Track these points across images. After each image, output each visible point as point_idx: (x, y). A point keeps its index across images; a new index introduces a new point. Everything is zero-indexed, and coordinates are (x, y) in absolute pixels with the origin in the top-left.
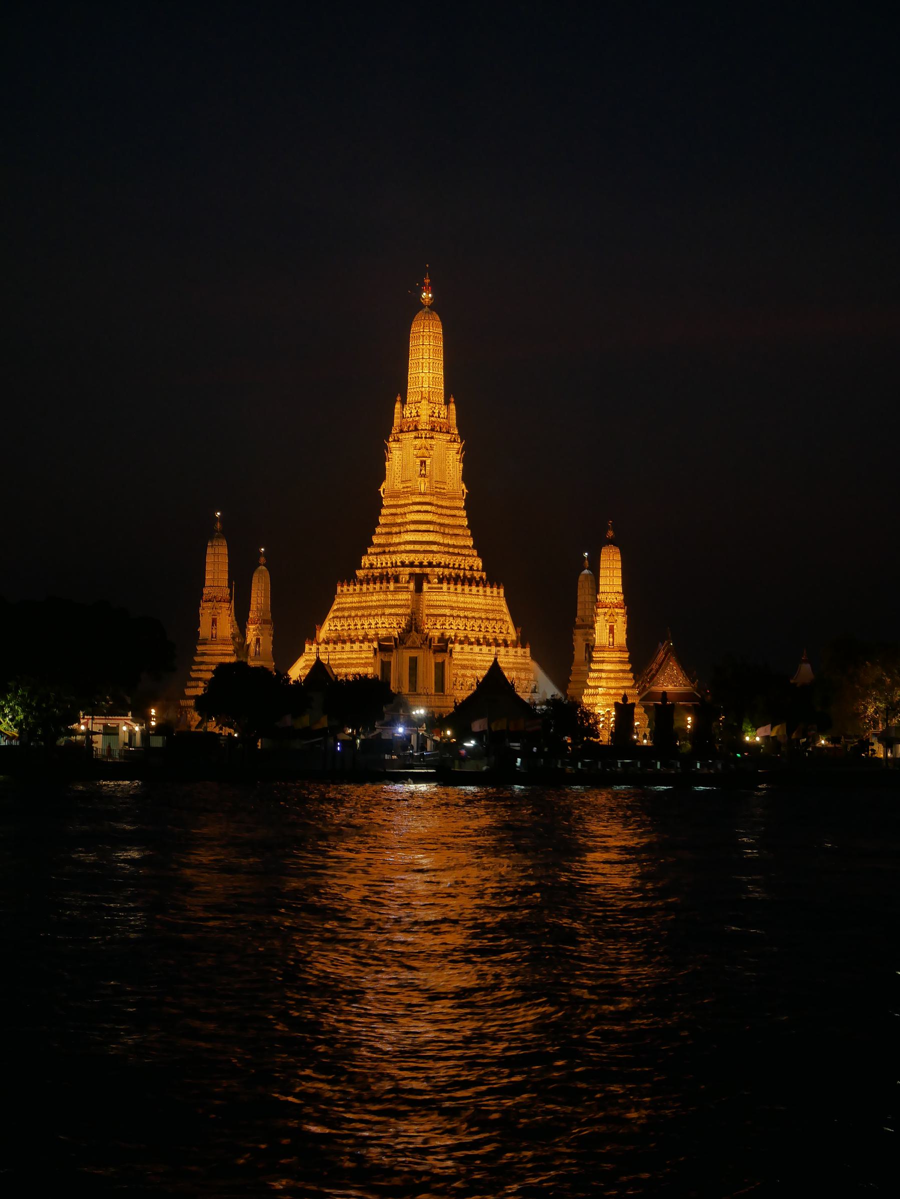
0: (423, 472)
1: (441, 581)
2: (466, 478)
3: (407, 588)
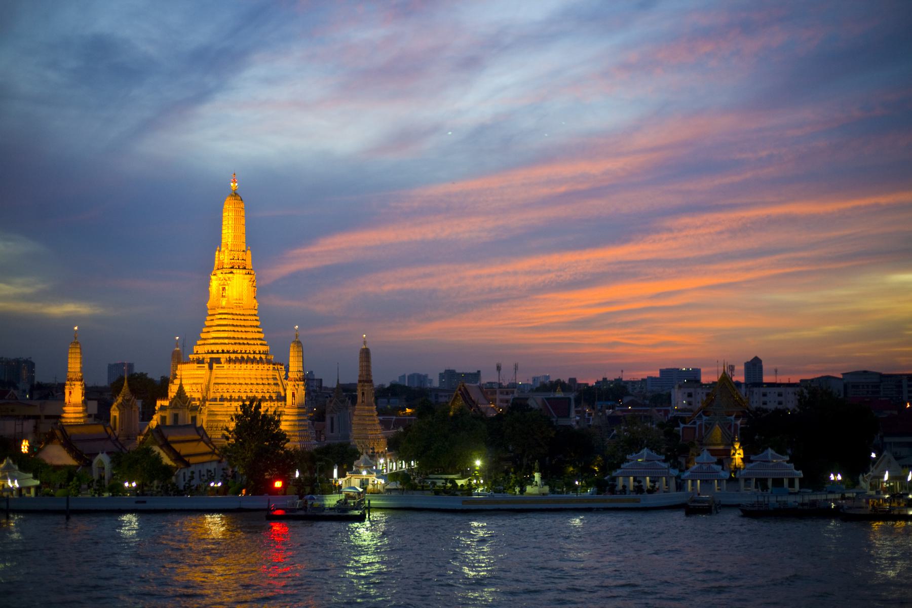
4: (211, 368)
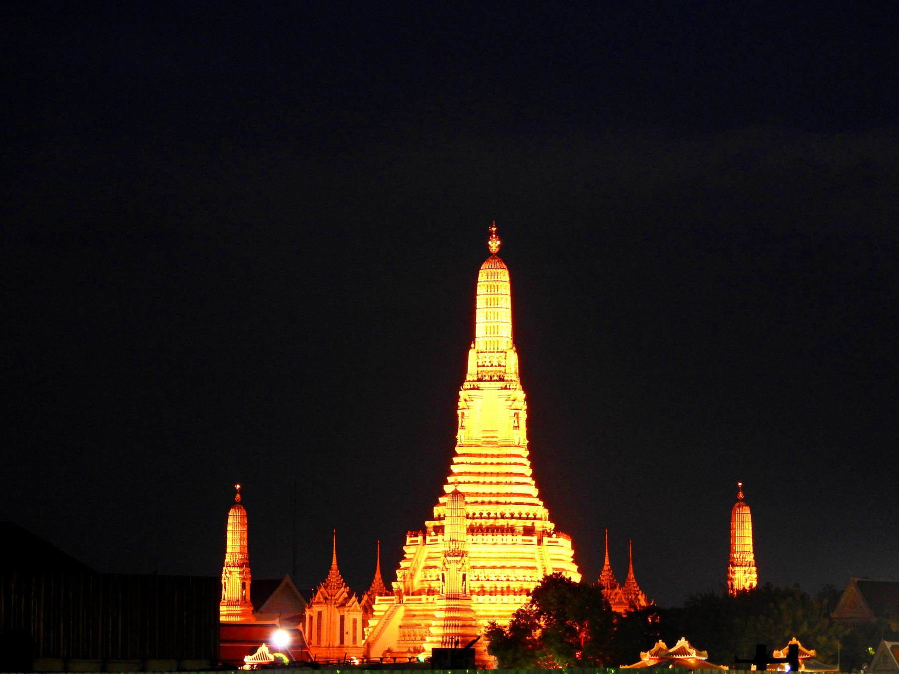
0: (516, 425)
3: (531, 541)
4: (540, 542)
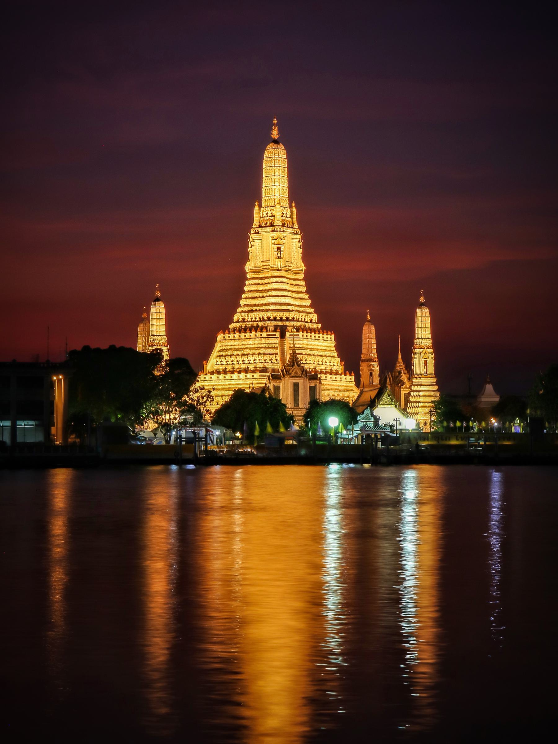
0: (279, 255)
1: (298, 330)
2: (304, 260)
3: (275, 335)
4: (283, 336)
